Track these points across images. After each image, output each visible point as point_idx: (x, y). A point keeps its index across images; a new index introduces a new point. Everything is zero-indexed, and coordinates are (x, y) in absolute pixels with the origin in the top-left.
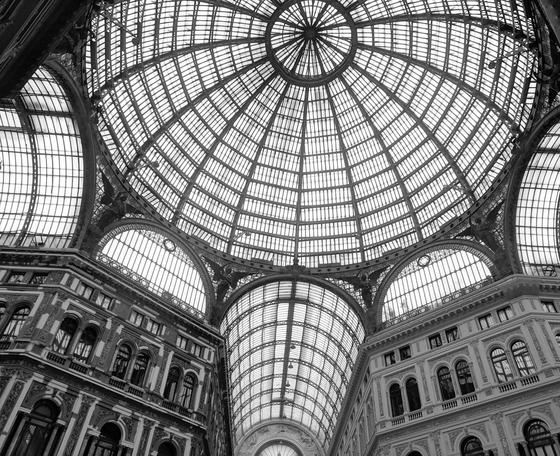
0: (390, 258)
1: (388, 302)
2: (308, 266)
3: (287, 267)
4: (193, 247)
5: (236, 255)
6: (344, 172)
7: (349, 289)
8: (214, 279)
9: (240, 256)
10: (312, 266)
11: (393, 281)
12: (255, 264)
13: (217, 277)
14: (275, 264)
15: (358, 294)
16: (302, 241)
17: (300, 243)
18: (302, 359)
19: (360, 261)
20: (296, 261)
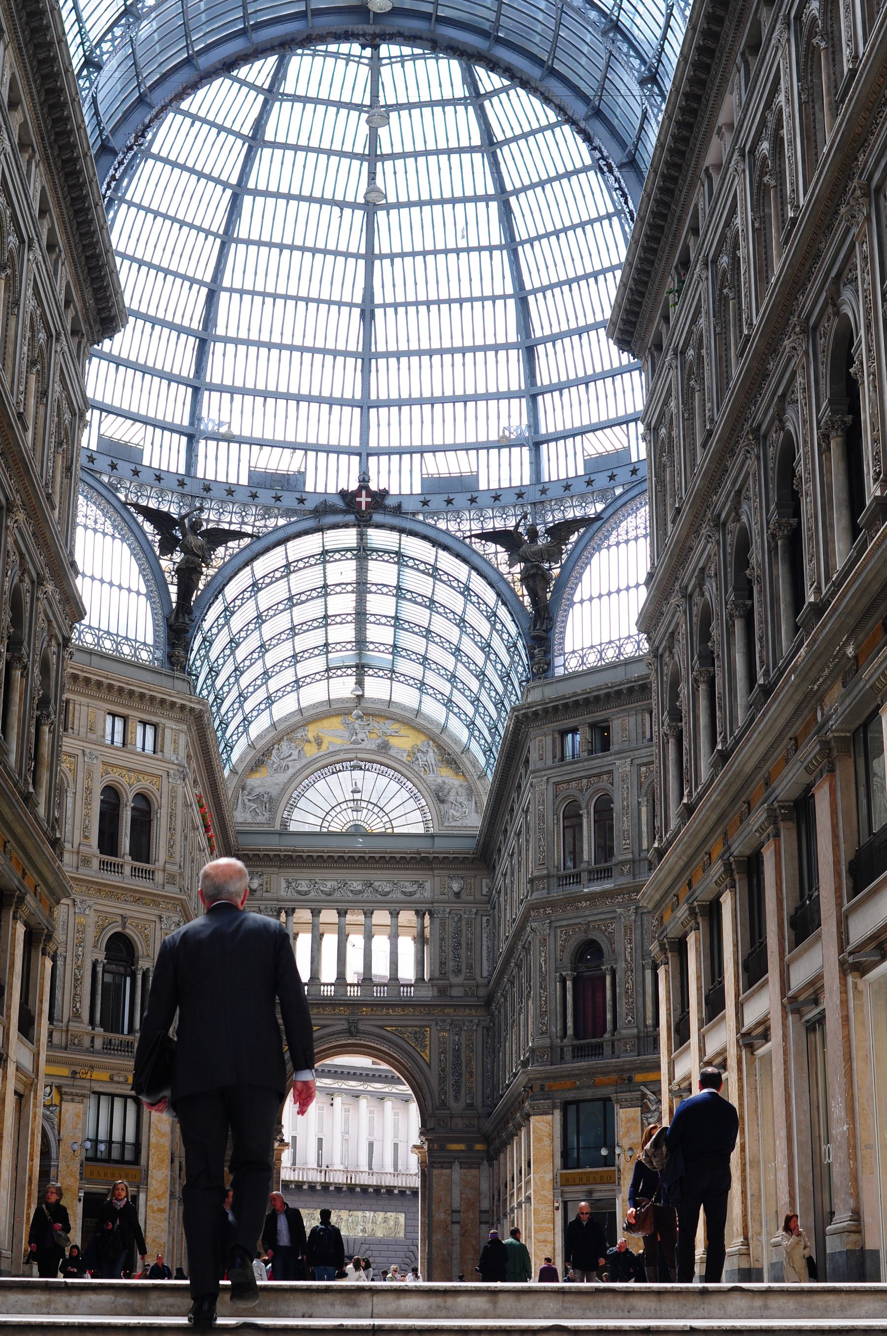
0: (597, 485)
1: (582, 602)
2: (394, 491)
3: (343, 494)
4: (105, 479)
5: (210, 476)
6: (494, 205)
7: (496, 553)
8: (163, 553)
9: (222, 478)
10: (406, 491)
11: (599, 549)
12: (261, 492)
13: (168, 546)
14: (309, 488)
15: (518, 568)
16: (377, 407)
17: (373, 411)
18: (399, 644)
19: (526, 481)
20: (364, 480)
